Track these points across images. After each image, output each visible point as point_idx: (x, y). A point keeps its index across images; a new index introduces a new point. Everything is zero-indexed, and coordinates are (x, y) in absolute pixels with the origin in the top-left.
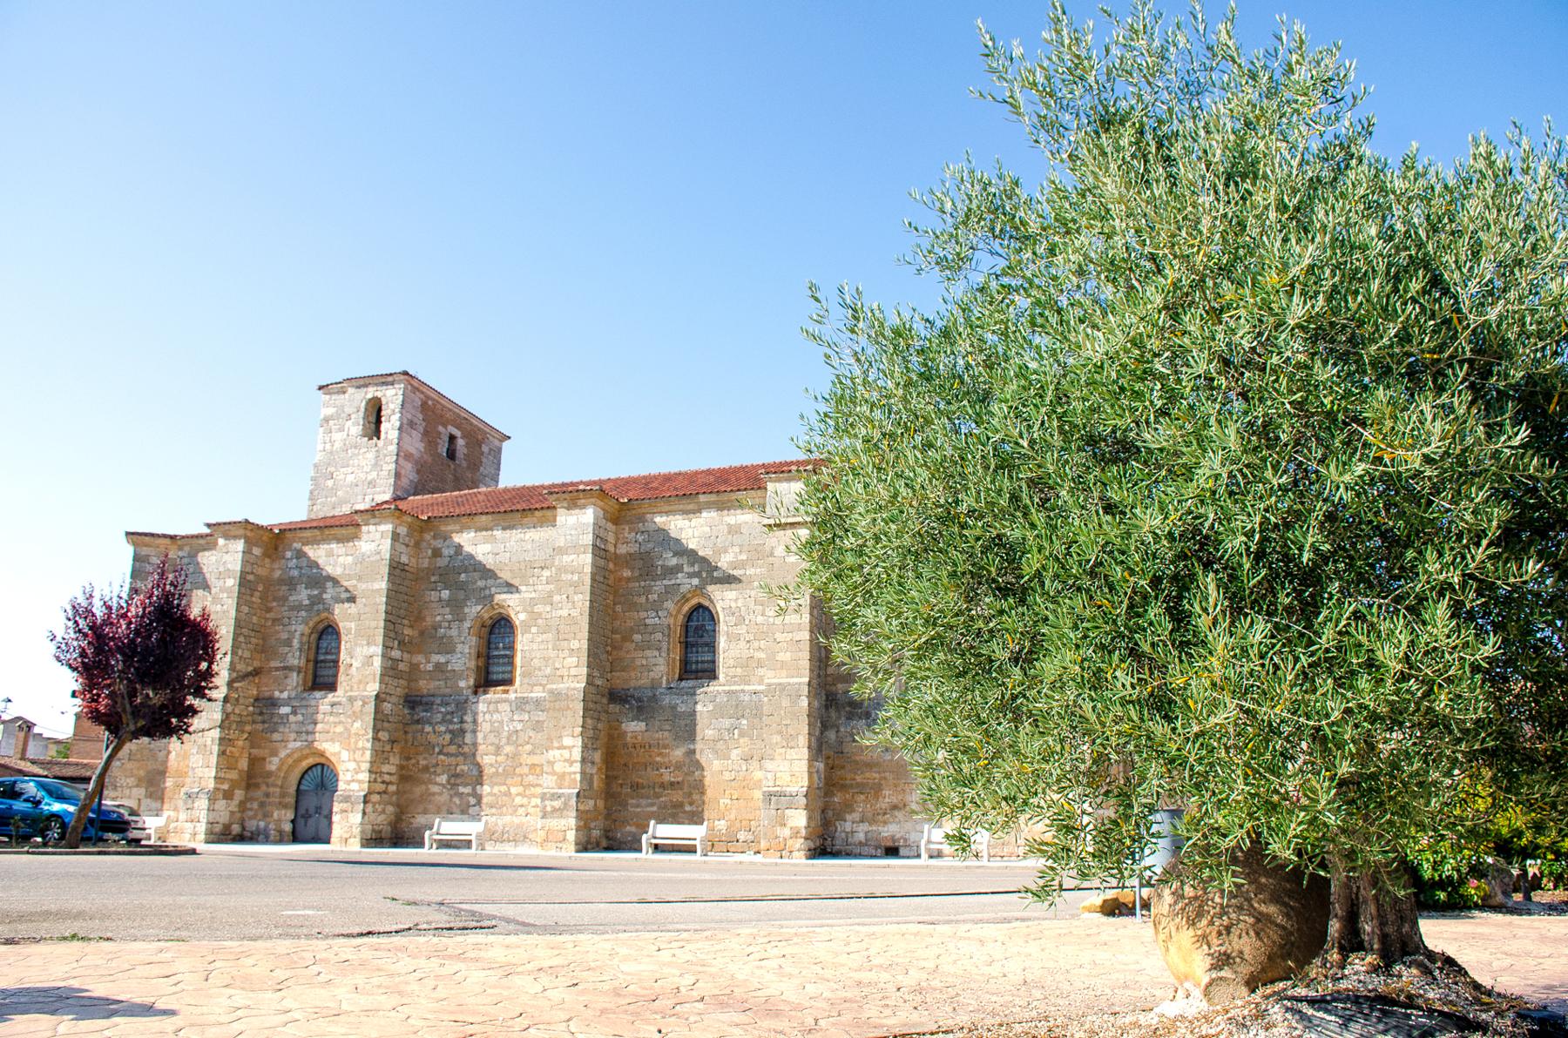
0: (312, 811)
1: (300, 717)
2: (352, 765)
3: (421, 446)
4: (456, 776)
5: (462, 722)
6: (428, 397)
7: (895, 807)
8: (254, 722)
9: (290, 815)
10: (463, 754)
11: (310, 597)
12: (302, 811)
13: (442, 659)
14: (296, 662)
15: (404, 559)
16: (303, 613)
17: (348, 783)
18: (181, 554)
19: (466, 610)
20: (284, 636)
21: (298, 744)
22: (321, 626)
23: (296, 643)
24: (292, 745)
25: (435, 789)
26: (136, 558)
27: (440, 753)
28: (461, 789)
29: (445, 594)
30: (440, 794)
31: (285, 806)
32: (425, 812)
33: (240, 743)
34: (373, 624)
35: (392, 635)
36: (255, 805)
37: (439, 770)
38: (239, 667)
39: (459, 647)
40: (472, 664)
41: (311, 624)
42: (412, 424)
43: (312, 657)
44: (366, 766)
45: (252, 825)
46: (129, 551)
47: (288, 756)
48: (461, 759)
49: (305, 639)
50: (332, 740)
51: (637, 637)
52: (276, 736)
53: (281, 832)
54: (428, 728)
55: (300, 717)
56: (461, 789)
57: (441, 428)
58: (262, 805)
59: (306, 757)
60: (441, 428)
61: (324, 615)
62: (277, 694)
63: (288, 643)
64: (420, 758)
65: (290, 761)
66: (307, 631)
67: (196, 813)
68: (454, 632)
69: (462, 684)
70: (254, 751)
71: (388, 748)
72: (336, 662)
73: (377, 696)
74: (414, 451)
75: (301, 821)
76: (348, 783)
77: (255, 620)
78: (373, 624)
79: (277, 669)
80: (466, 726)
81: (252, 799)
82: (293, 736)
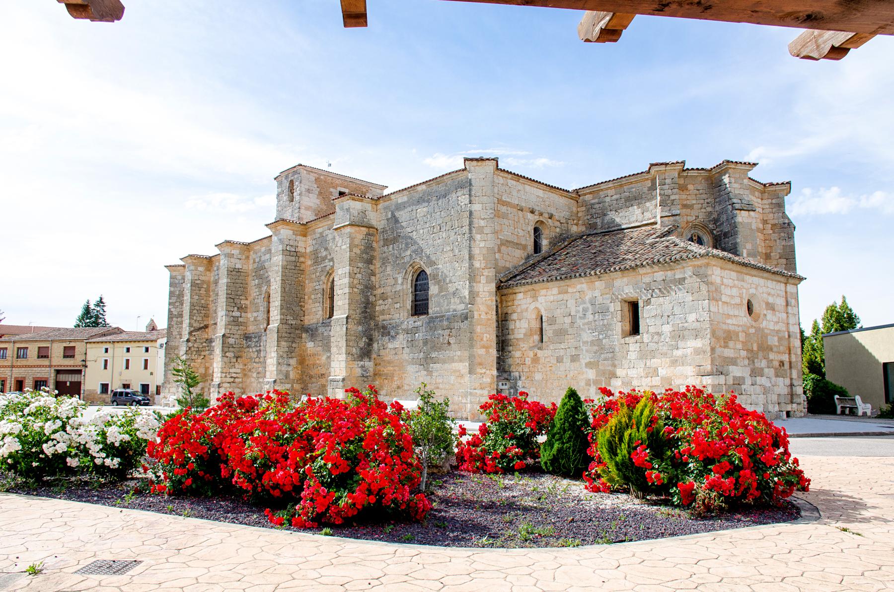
3: (318, 201)
6: (321, 175)
7: (399, 387)
15: (238, 266)
26: (171, 278)
33: (199, 361)
35: (233, 305)
38: (195, 325)
42: (308, 191)
46: (167, 274)
51: (313, 297)
57: (332, 190)
60: (332, 190)
71: (235, 360)
73: (224, 336)
74: (312, 205)
77: (203, 302)
80: (262, 348)
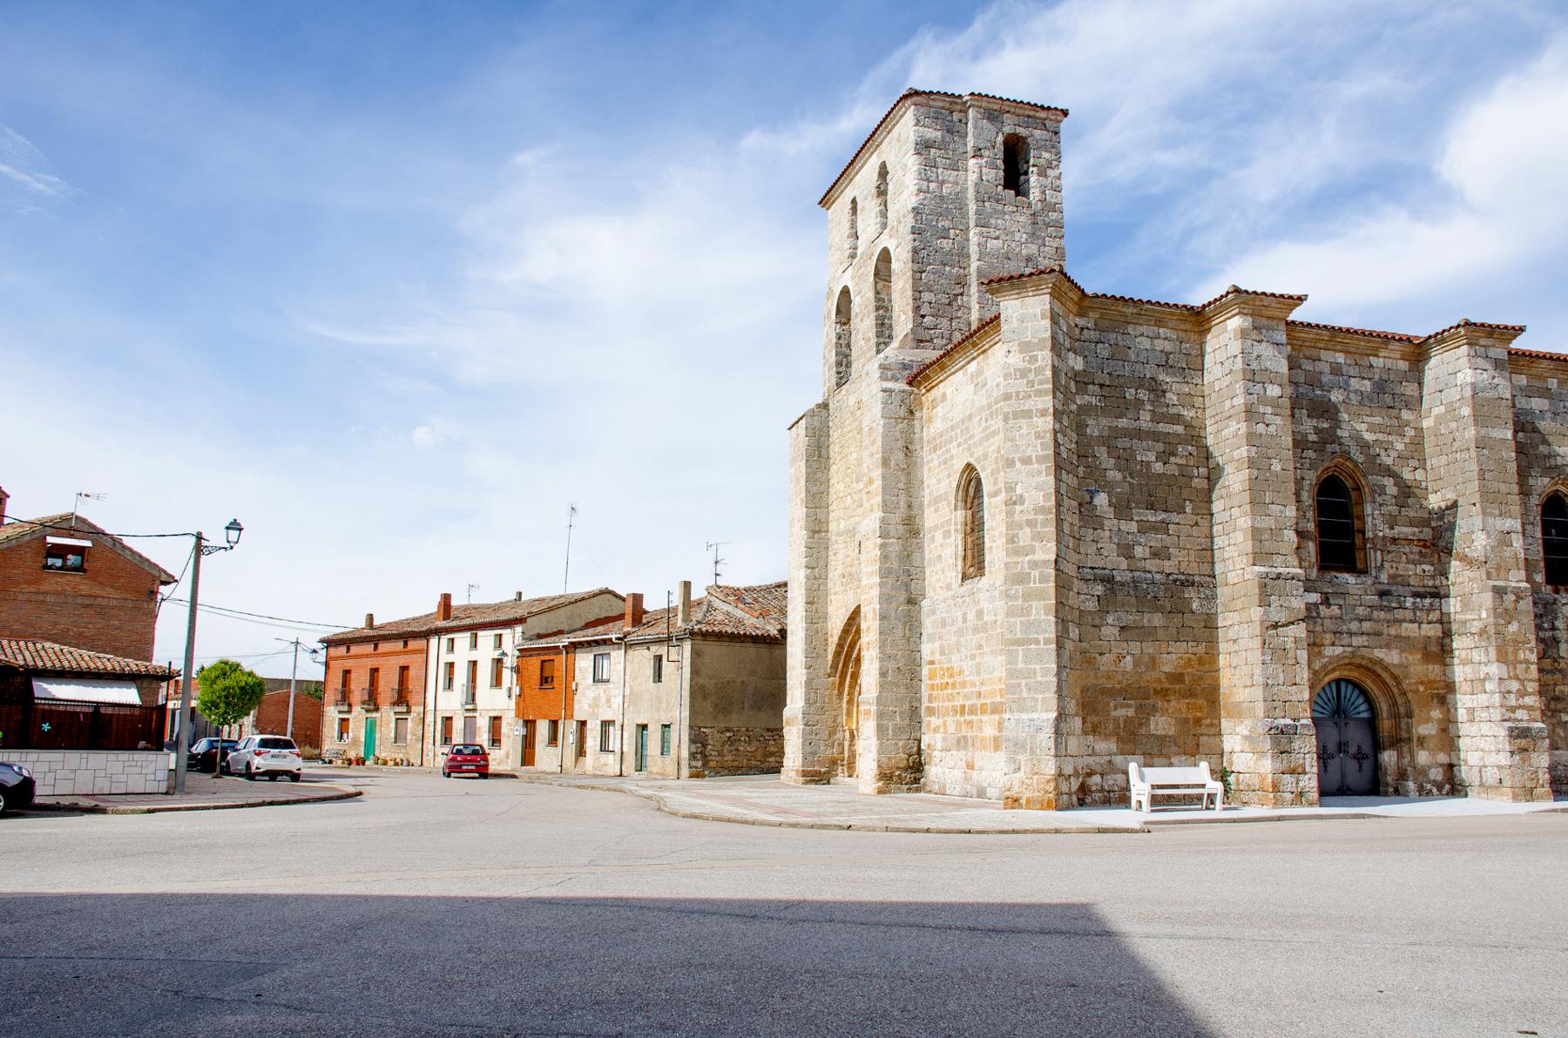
1: (1335, 610)
4: (1557, 699)
11: (1317, 431)
16: (1310, 454)
18: (1082, 322)
21: (1339, 650)
34: (1504, 488)
44: (1532, 687)
50: (1388, 646)
55: (1335, 610)
67: (1297, 759)
82: (1328, 638)
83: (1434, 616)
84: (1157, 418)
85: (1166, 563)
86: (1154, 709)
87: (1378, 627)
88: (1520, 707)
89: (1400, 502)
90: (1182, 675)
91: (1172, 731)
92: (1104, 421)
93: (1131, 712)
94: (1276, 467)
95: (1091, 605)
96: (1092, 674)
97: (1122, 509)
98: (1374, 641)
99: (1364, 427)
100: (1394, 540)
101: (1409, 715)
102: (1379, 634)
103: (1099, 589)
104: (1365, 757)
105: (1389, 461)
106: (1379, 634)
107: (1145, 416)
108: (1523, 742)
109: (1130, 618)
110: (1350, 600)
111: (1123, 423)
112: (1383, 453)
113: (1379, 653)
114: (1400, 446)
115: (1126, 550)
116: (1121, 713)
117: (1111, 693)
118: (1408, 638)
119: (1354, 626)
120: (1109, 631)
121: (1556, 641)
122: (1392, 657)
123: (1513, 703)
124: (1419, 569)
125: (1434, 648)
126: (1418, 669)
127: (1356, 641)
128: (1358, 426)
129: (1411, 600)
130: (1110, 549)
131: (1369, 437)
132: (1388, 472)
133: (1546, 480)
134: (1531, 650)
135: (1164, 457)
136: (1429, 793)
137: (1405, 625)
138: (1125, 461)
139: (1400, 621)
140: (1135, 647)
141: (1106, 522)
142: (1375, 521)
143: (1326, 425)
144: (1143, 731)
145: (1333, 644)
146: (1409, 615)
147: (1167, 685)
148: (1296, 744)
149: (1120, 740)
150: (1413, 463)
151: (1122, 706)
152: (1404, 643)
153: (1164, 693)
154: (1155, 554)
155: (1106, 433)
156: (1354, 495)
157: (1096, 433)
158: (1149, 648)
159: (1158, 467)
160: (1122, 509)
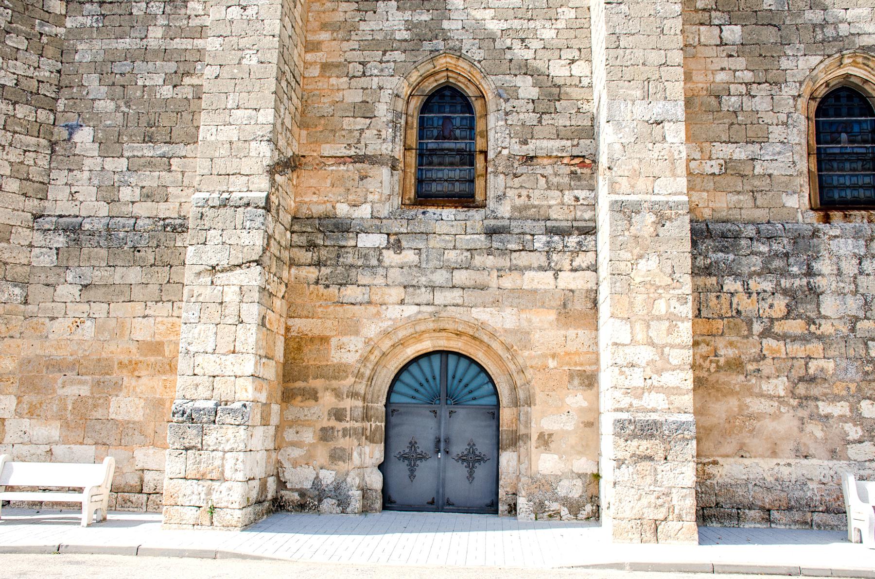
0: (425, 444)
1: (409, 256)
2: (645, 354)
5: (810, 273)
8: (293, 263)
9: (377, 453)
10: (819, 338)
11: (410, 26)
12: (401, 446)
13: (740, 153)
14: (386, 148)
16: (398, 56)
17: (639, 393)
19: (785, 63)
20: (355, 97)
21: (410, 310)
22: (430, 85)
23: (382, 111)
24: (394, 312)
25: (756, 405)
27: (766, 333)
28: (824, 408)
29: (733, 33)
30: (775, 417)
31: (371, 440)
32: (742, 452)
36: (309, 436)
37: (767, 367)
39: (777, 133)
40: (803, 165)
41: (415, 77)
43: (413, 140)
45: (301, 477)
47: (386, 334)
48: (815, 347)
49: (400, 105)
50: (496, 303)
52: (351, 293)
53: (365, 492)
54: (730, 285)
56: (824, 408)
58: (326, 434)
59: (417, 336)
61: (442, 62)
62: (343, 210)
63: (365, 109)
64: (720, 343)
65: (386, 345)
66: (406, 91)
67: (210, 461)
68: (761, 103)
69: (792, 202)
70: (299, 325)
72: (468, 158)
75: (400, 469)
76: (639, 393)
78: (655, 57)
79: (341, 160)
80: (820, 282)
81: (295, 423)
82: (396, 293)
83: (583, 260)
84: (170, 34)
85: (162, 205)
86: (118, 386)
87: (480, 278)
88: (651, 389)
89: (541, 108)
90: (160, 344)
91: (138, 416)
92: (98, 44)
93: (85, 391)
94: (251, 60)
95: (47, 260)
96: (37, 343)
97: (108, 145)
98: (471, 296)
99: (489, 13)
100: (529, 159)
101: (529, 402)
102: (483, 288)
103: (60, 240)
104: (480, 459)
105: (528, 55)
106: (483, 288)
107: (156, 33)
108: (644, 446)
109: (97, 276)
110: (434, 242)
111: (125, 44)
112: (517, 45)
113: (480, 314)
114: (548, 34)
115: (109, 194)
116: (72, 391)
117: (56, 366)
118: (535, 291)
119: (440, 277)
120: (68, 291)
121: (814, 293)
122: (501, 319)
123: (640, 383)
124: (568, 197)
125: (580, 305)
126: (545, 332)
127: (440, 298)
128: (478, 14)
129: (544, 238)
130: (87, 193)
131: (494, 26)
132: (525, 69)
133: (814, 60)
134: (682, 299)
135: (175, 79)
136: (554, 515)
137: (529, 274)
138: (120, 90)
139: (522, 270)
140: (99, 310)
141: (87, 162)
142: (497, 135)
143: (425, 17)
144: (99, 414)
145: (402, 302)
146: (538, 259)
147: (137, 357)
148: (210, 440)
149: (66, 425)
150: (567, 54)
151: (72, 383)
152: (529, 298)
153: (132, 367)
154: (148, 196)
155: (99, 58)
156: (477, 105)
157: (88, 58)
158: (119, 309)
159: (167, 91)
160: (108, 145)
